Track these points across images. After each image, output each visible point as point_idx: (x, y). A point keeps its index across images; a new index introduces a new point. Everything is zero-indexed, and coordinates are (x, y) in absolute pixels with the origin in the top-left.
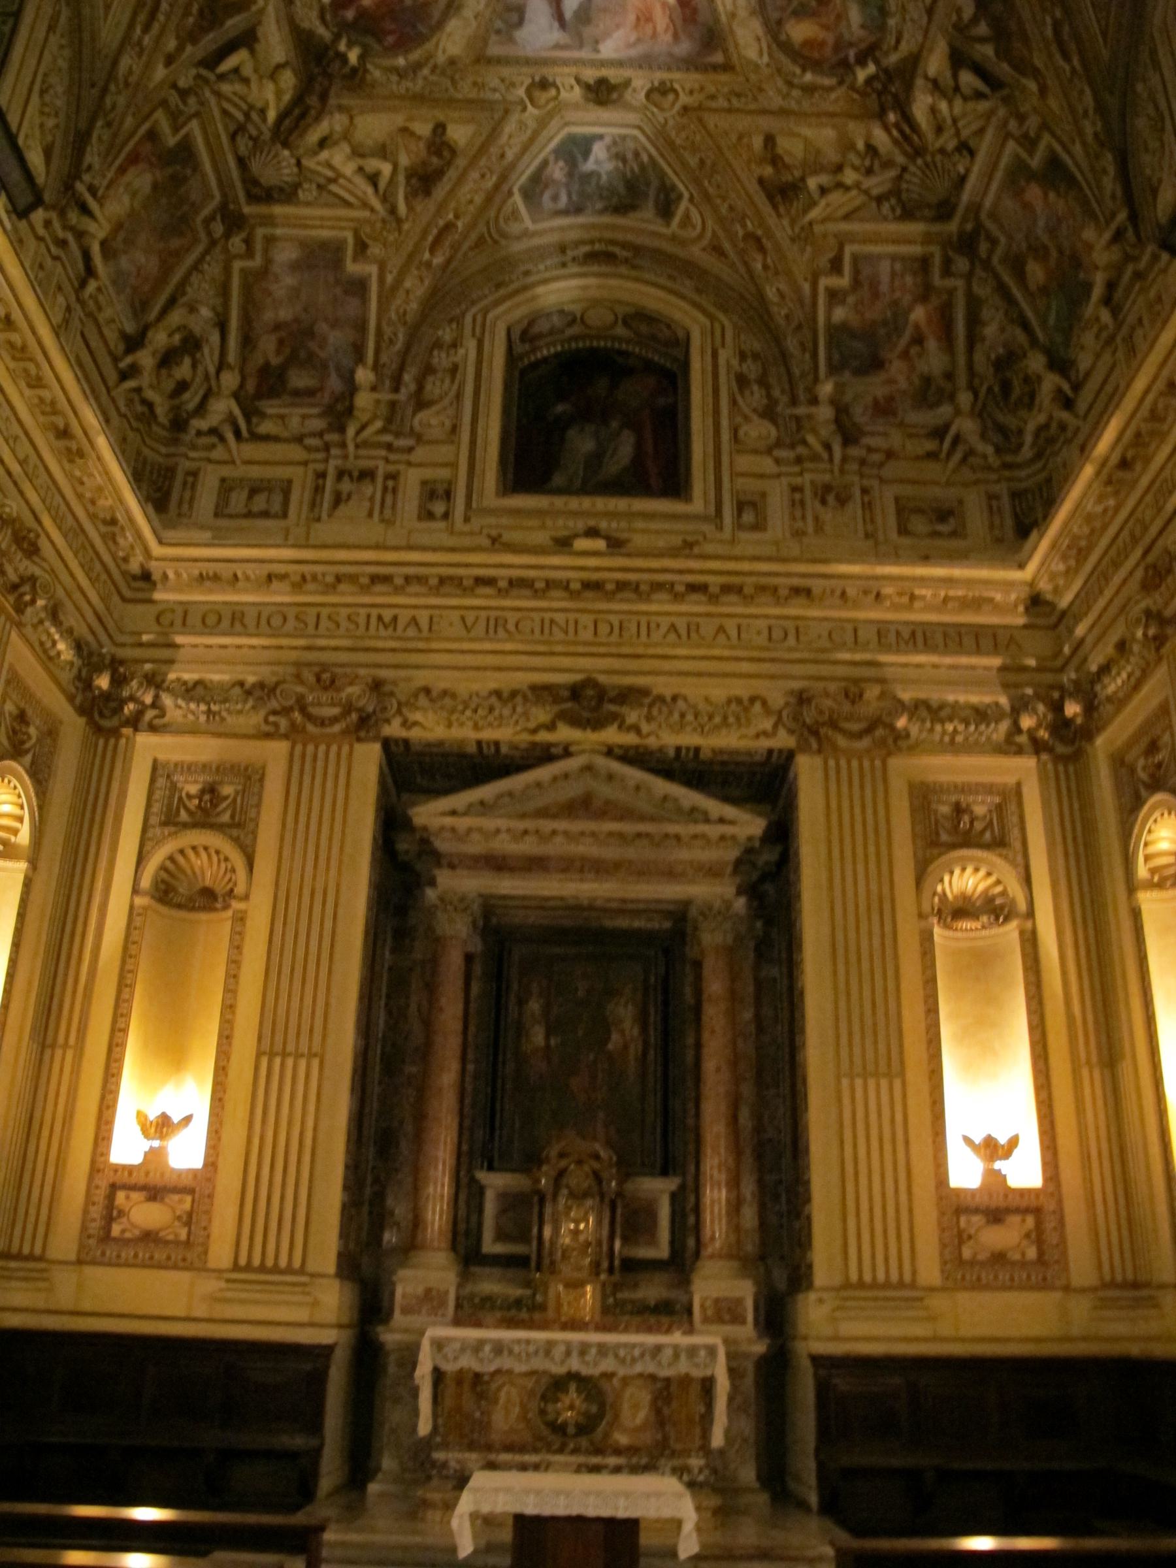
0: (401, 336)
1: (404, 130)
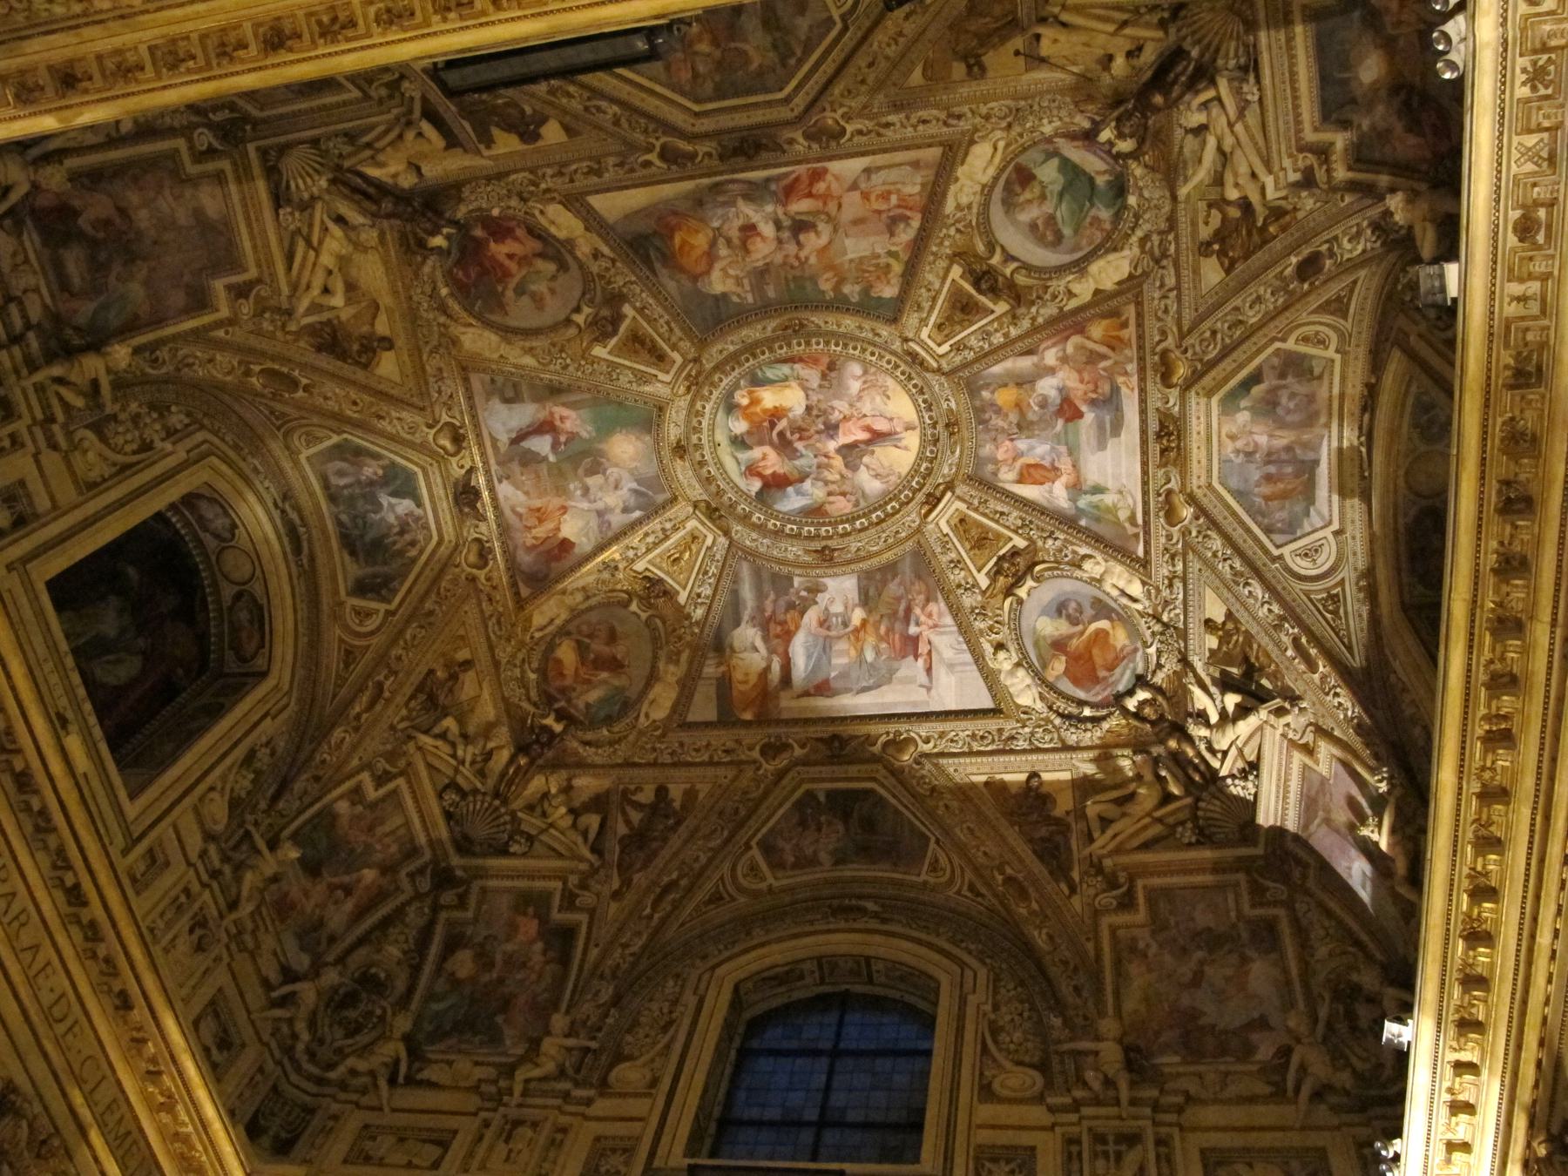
0: (164, 370)
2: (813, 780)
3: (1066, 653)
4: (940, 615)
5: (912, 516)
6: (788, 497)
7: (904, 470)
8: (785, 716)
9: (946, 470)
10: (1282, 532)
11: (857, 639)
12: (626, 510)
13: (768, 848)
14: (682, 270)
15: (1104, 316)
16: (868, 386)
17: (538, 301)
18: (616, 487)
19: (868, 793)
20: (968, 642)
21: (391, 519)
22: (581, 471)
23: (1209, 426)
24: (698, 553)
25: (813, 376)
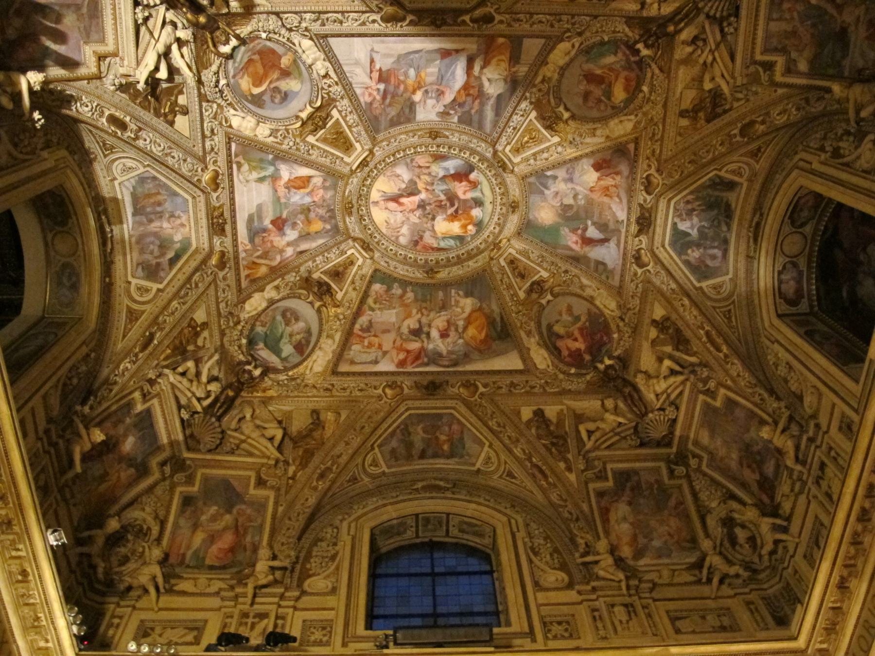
0: (762, 392)
1: (654, 343)
3: (281, 69)
4: (363, 94)
6: (454, 168)
8: (476, 39)
9: (355, 180)
10: (148, 178)
11: (419, 83)
12: (555, 178)
14: (485, 314)
15: (259, 278)
16: (397, 229)
17: (570, 309)
18: (557, 193)
21: (695, 220)
22: (575, 209)
23: (197, 231)
24: (517, 141)
25: (428, 239)
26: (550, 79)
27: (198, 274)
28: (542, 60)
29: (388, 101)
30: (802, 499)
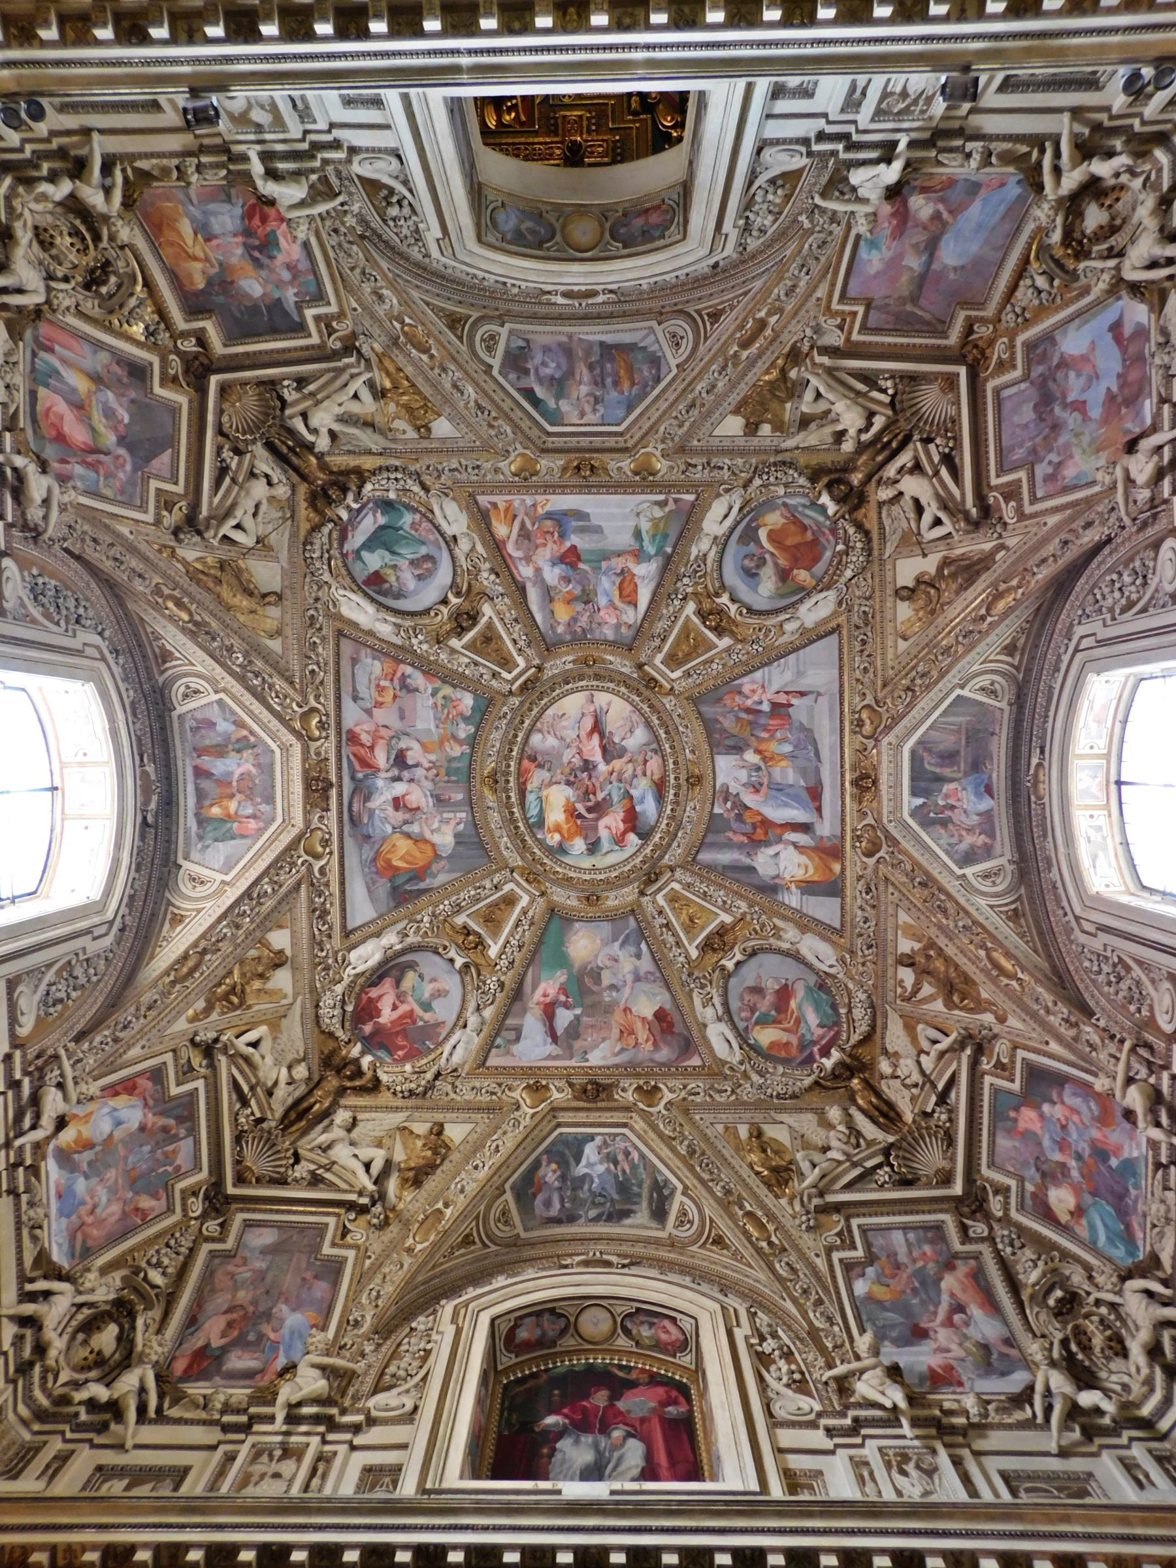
0: (368, 1318)
2: (898, 807)
3: (791, 570)
4: (753, 682)
5: (669, 702)
7: (630, 708)
10: (659, 369)
11: (772, 759)
12: (638, 956)
13: (968, 859)
14: (428, 866)
16: (553, 730)
17: (440, 994)
19: (913, 753)
20: (779, 658)
21: (601, 1168)
22: (595, 988)
24: (687, 898)
26: (780, 938)
27: (509, 430)
28: (806, 924)
29: (744, 715)
30: (211, 1435)
